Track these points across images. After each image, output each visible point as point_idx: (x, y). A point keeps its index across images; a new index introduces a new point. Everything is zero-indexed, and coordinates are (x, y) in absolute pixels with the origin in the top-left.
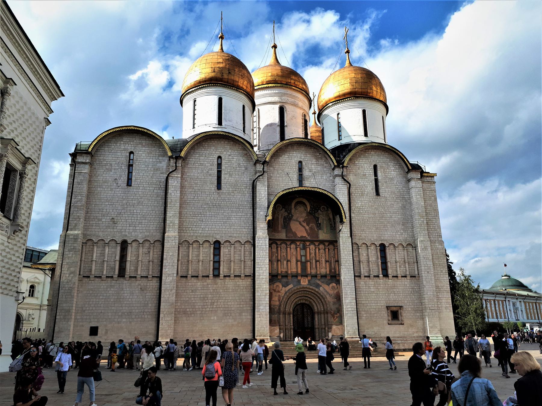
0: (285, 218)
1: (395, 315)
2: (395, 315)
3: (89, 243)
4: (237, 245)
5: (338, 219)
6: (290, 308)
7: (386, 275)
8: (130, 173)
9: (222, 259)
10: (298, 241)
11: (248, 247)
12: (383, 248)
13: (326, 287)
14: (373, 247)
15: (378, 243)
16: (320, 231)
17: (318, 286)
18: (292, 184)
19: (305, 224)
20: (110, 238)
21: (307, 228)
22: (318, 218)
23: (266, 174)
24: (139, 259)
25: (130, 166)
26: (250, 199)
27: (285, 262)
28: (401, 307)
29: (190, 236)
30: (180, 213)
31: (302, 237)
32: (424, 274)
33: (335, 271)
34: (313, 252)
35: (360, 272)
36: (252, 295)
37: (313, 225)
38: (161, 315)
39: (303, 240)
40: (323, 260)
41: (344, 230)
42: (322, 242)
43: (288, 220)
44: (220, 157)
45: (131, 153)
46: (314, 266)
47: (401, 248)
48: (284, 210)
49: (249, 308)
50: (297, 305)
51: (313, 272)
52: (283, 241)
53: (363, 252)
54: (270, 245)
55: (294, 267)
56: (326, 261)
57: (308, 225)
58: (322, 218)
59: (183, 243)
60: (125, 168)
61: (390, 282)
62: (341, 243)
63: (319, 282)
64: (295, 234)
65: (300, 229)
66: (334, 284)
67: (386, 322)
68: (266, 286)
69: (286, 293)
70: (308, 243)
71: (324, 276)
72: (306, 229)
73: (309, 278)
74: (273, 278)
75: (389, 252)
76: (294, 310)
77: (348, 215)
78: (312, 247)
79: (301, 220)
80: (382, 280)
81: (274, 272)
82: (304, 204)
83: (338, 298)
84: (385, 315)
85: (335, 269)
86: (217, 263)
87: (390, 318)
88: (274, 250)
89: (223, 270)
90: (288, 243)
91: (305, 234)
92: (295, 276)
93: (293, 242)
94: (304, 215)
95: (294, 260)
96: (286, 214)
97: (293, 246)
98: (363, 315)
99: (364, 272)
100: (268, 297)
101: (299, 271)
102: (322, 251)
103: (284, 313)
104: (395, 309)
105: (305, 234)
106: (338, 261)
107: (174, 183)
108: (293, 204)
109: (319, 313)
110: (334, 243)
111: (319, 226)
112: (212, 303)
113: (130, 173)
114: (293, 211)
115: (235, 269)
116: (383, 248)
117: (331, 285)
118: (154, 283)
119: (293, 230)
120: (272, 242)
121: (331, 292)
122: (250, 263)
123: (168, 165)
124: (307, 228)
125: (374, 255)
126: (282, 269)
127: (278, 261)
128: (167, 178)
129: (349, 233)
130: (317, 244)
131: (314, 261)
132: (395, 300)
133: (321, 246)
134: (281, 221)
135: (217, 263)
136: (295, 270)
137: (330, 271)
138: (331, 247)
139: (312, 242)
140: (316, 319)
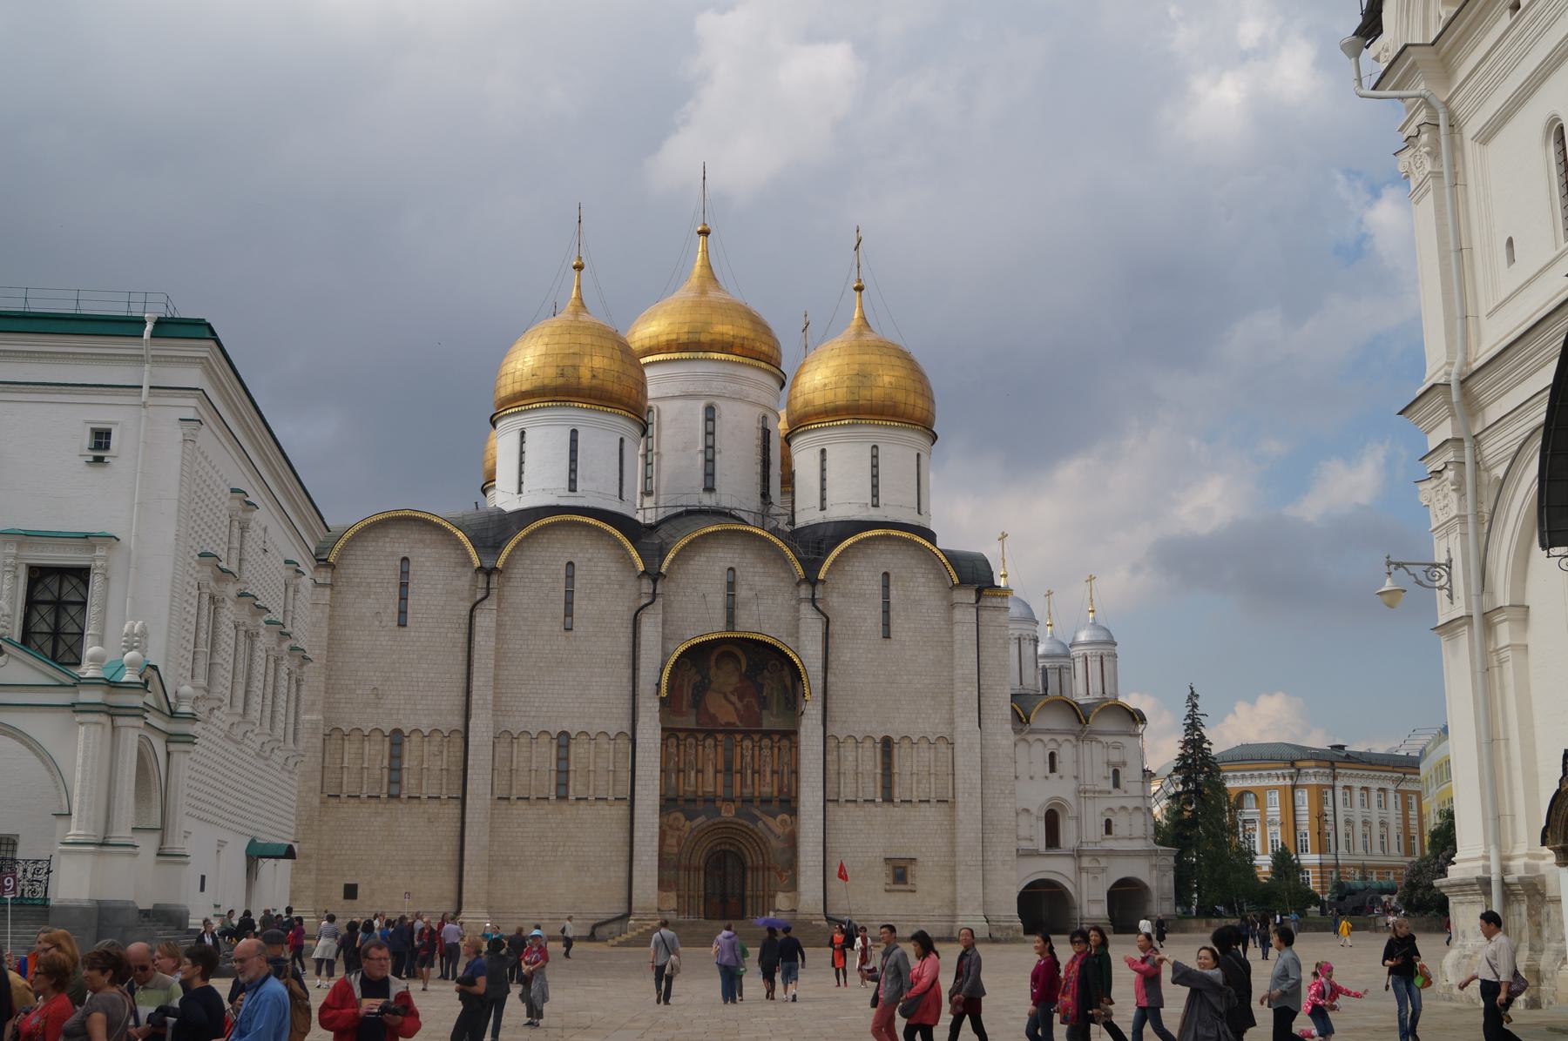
1: (900, 872)
2: (900, 872)
3: (337, 735)
4: (602, 739)
6: (699, 859)
7: (888, 799)
8: (403, 598)
9: (572, 768)
11: (624, 745)
14: (868, 744)
16: (764, 712)
17: (755, 819)
18: (711, 626)
19: (734, 699)
20: (372, 726)
21: (739, 705)
22: (762, 686)
23: (659, 600)
24: (426, 765)
25: (404, 586)
27: (693, 774)
29: (515, 724)
30: (496, 678)
31: (728, 724)
32: (960, 798)
33: (790, 791)
35: (839, 794)
36: (627, 835)
38: (466, 868)
39: (730, 732)
40: (768, 769)
41: (811, 712)
42: (768, 734)
43: (700, 691)
44: (571, 564)
45: (405, 559)
46: (749, 782)
48: (693, 670)
49: (624, 858)
51: (747, 792)
53: (849, 754)
54: (664, 740)
55: (711, 783)
56: (773, 772)
57: (741, 699)
59: (503, 736)
60: (394, 591)
61: (897, 812)
63: (757, 812)
64: (713, 718)
65: (724, 710)
66: (786, 816)
69: (692, 830)
70: (738, 737)
71: (766, 801)
72: (736, 709)
73: (738, 804)
74: (668, 803)
77: (817, 683)
78: (748, 743)
79: (730, 688)
81: (672, 794)
82: (736, 658)
83: (792, 842)
84: (882, 874)
85: (789, 786)
86: (563, 774)
87: (890, 880)
88: (673, 750)
89: (576, 787)
90: (701, 737)
91: (734, 719)
92: (710, 800)
93: (710, 733)
94: (734, 679)
95: (710, 771)
97: (710, 742)
99: (847, 792)
100: (657, 839)
101: (720, 791)
102: (766, 752)
103: (688, 869)
104: (902, 864)
105: (734, 719)
106: (795, 772)
107: (485, 621)
108: (713, 658)
109: (755, 869)
110: (791, 735)
111: (764, 703)
113: (403, 598)
114: (712, 672)
116: (887, 743)
117: (779, 818)
118: (453, 809)
119: (712, 711)
120: (668, 733)
121: (779, 830)
122: (625, 775)
123: (474, 585)
124: (739, 705)
125: (870, 761)
126: (690, 784)
127: (679, 771)
128: (472, 611)
129: (820, 717)
130: (756, 738)
133: (766, 742)
134: (687, 692)
135: (563, 774)
136: (711, 789)
137: (780, 791)
138: (785, 743)
139: (747, 734)
140: (749, 881)
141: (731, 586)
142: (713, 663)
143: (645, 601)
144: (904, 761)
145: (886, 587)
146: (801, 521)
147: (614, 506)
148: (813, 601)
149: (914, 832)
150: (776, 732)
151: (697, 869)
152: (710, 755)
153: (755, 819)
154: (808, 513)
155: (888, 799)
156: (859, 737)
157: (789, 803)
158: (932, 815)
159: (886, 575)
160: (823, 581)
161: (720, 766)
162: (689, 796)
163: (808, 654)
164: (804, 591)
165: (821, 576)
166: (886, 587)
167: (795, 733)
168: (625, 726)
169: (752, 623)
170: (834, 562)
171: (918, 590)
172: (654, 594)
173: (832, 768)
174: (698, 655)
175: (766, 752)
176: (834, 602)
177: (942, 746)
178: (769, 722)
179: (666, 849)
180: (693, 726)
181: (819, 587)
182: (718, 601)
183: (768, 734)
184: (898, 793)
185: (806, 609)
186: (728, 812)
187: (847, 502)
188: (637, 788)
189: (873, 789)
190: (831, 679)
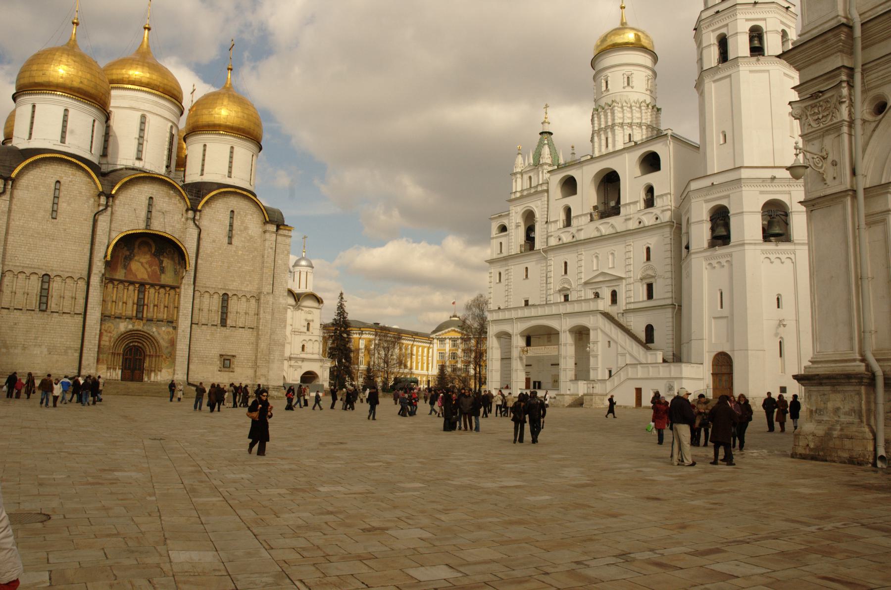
1: (227, 362)
2: (227, 362)
10: (137, 283)
11: (82, 284)
12: (225, 298)
15: (221, 292)
18: (137, 225)
19: (147, 266)
23: (109, 209)
26: (90, 233)
27: (121, 304)
28: (233, 356)
33: (173, 317)
37: (157, 268)
39: (142, 285)
42: (163, 286)
47: (244, 299)
51: (150, 315)
52: (121, 282)
57: (150, 266)
61: (226, 331)
62: (183, 290)
67: (216, 368)
70: (147, 287)
74: (105, 317)
75: (233, 305)
76: (124, 351)
77: (193, 262)
78: (152, 290)
80: (220, 329)
81: (107, 313)
83: (173, 343)
85: (173, 315)
90: (126, 284)
91: (146, 277)
93: (132, 283)
96: (128, 253)
97: (131, 288)
98: (194, 359)
101: (134, 314)
102: (162, 295)
105: (146, 277)
108: (137, 243)
112: (36, 338)
114: (136, 251)
115: (67, 305)
116: (225, 298)
122: (82, 301)
124: (149, 270)
125: (216, 302)
130: (157, 288)
131: (152, 305)
132: (229, 350)
133: (162, 291)
138: (172, 292)
139: (152, 285)
141: (150, 205)
142: (136, 246)
143: (101, 208)
144: (234, 305)
145: (232, 218)
146: (189, 180)
147: (87, 156)
148: (194, 219)
149: (238, 343)
150: (168, 286)
151: (119, 354)
152: (131, 295)
154: (193, 175)
155: (224, 323)
156: (212, 292)
157: (172, 323)
158: (247, 334)
159: (232, 212)
160: (200, 211)
161: (136, 301)
162: (117, 315)
163: (190, 247)
164: (191, 214)
165: (199, 208)
166: (232, 218)
167: (178, 287)
168: (85, 274)
169: (158, 226)
170: (207, 202)
171: (250, 222)
172: (107, 206)
173: (196, 306)
175: (162, 295)
176: (204, 223)
177: (253, 301)
179: (102, 343)
180: (123, 278)
181: (198, 213)
182: (143, 214)
183: (163, 286)
184: (229, 322)
185: (191, 223)
187: (215, 173)
188: (88, 308)
189: (217, 319)
190: (199, 261)
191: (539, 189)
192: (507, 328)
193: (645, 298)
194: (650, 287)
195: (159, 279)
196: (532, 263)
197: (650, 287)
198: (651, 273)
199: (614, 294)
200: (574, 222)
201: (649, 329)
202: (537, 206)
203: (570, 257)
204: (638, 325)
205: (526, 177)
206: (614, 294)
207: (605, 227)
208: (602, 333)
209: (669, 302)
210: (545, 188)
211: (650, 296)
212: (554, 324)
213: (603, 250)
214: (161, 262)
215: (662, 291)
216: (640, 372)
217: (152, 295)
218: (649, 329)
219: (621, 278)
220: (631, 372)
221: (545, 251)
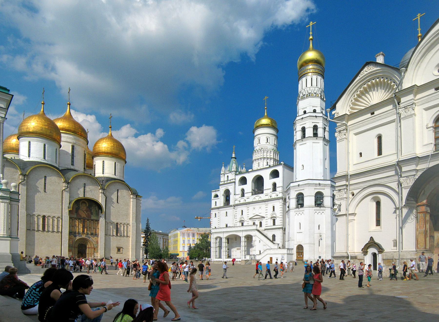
0: (76, 208)
5: (100, 211)
13: (93, 238)
34: (88, 224)
42: (92, 220)
50: (79, 244)
58: (93, 211)
68: (67, 237)
78: (88, 222)
91: (85, 216)
102: (92, 224)
103: (74, 247)
105: (85, 216)
110: (98, 221)
121: (95, 240)
133: (92, 222)
138: (96, 222)
153: (90, 238)
167: (99, 220)
174: (78, 202)
175: (92, 224)
178: (93, 217)
186: (84, 236)
191: (232, 181)
192: (221, 235)
193: (272, 224)
194: (274, 221)
195: (90, 217)
196: (230, 210)
197: (274, 221)
198: (274, 215)
199: (261, 223)
200: (245, 195)
201: (274, 236)
202: (231, 188)
203: (244, 208)
204: (270, 234)
205: (226, 175)
206: (261, 223)
207: (257, 198)
208: (257, 238)
209: (281, 226)
210: (234, 181)
211: (274, 224)
212: (240, 234)
213: (257, 206)
214: (91, 210)
215: (278, 222)
216: (272, 252)
217: (88, 224)
218: (274, 236)
219: (264, 217)
220: (268, 252)
221: (235, 206)
